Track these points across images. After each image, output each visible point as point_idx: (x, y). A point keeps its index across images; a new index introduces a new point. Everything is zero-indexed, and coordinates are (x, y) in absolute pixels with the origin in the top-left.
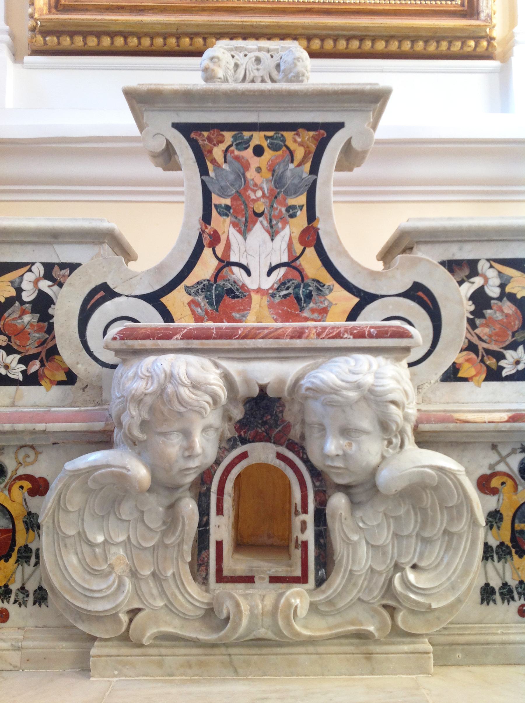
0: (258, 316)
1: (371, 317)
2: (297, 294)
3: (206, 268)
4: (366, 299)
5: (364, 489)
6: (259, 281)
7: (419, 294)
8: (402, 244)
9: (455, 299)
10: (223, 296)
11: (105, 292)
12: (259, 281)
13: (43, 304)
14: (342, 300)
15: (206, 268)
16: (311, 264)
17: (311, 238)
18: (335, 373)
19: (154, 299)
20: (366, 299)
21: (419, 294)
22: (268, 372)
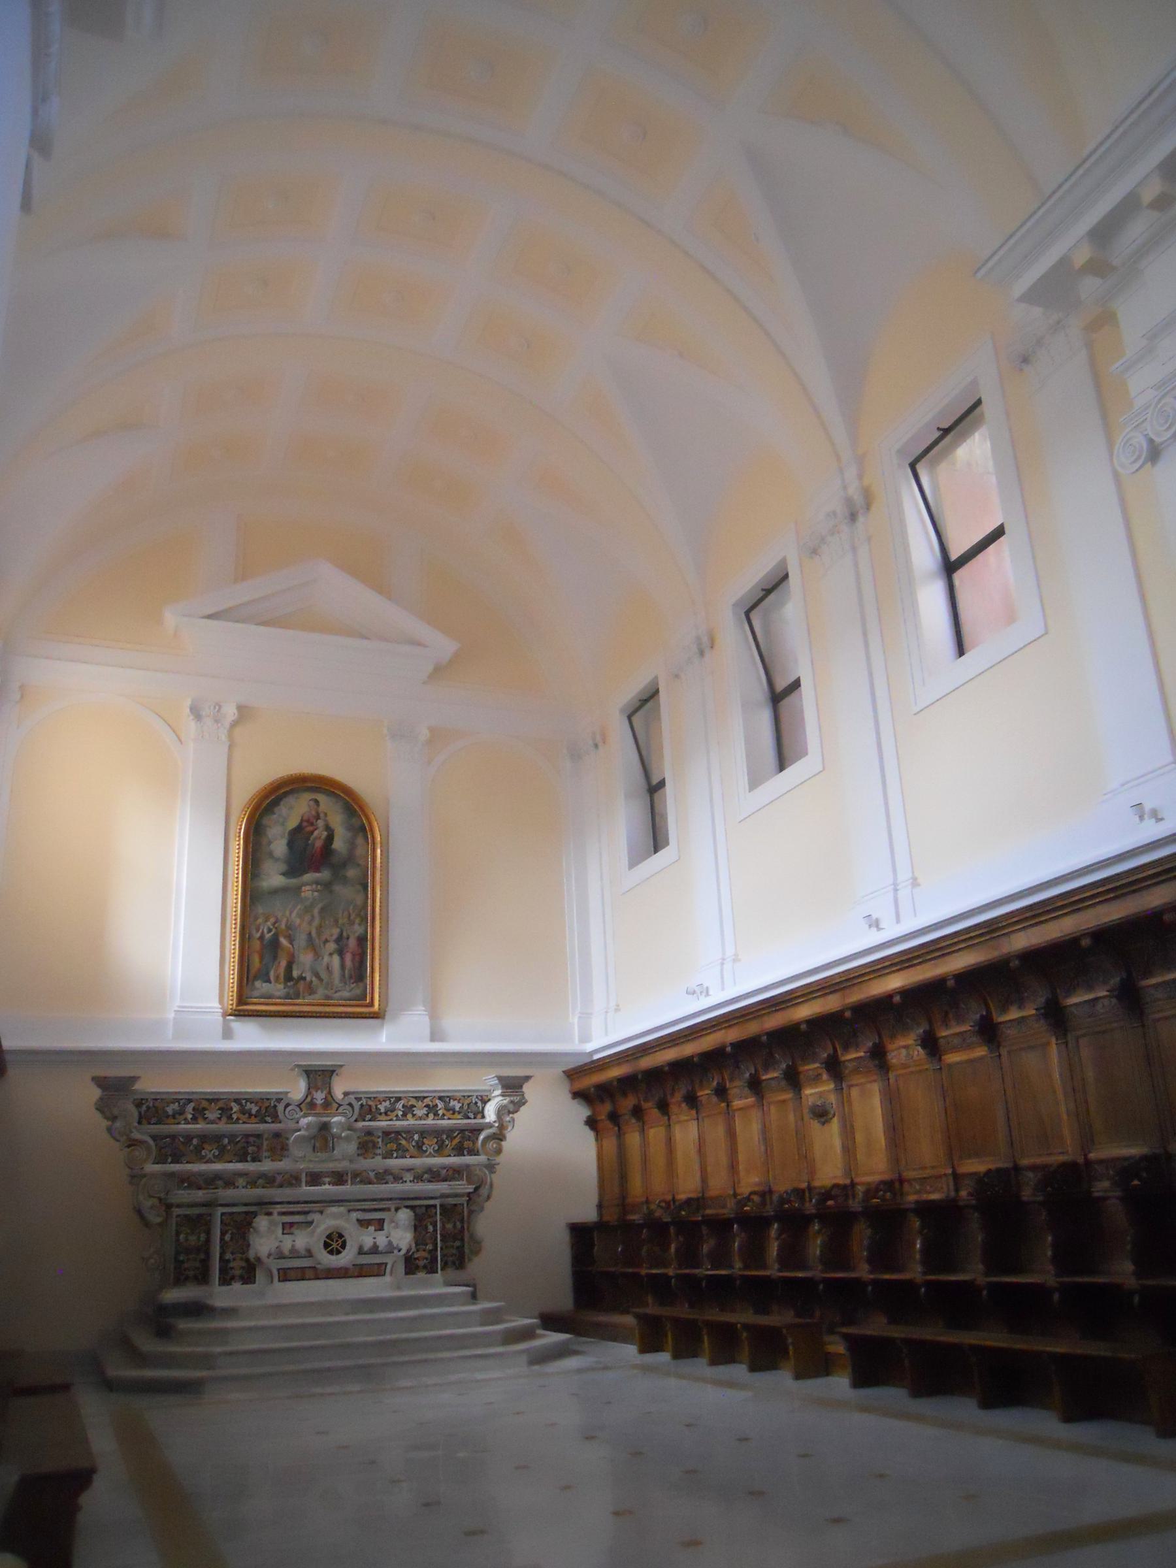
0: (319, 1110)
1: (340, 1110)
2: (327, 1104)
3: (309, 1099)
4: (340, 1105)
5: (340, 1137)
6: (319, 1102)
7: (350, 1105)
8: (346, 1094)
9: (357, 1105)
10: (312, 1105)
11: (288, 1105)
12: (319, 1102)
13: (275, 1106)
14: (335, 1106)
15: (309, 1099)
16: (329, 1098)
17: (330, 1093)
18: (335, 1119)
19: (299, 1106)
20: (340, 1105)
21: (350, 1105)
22: (325, 1119)
